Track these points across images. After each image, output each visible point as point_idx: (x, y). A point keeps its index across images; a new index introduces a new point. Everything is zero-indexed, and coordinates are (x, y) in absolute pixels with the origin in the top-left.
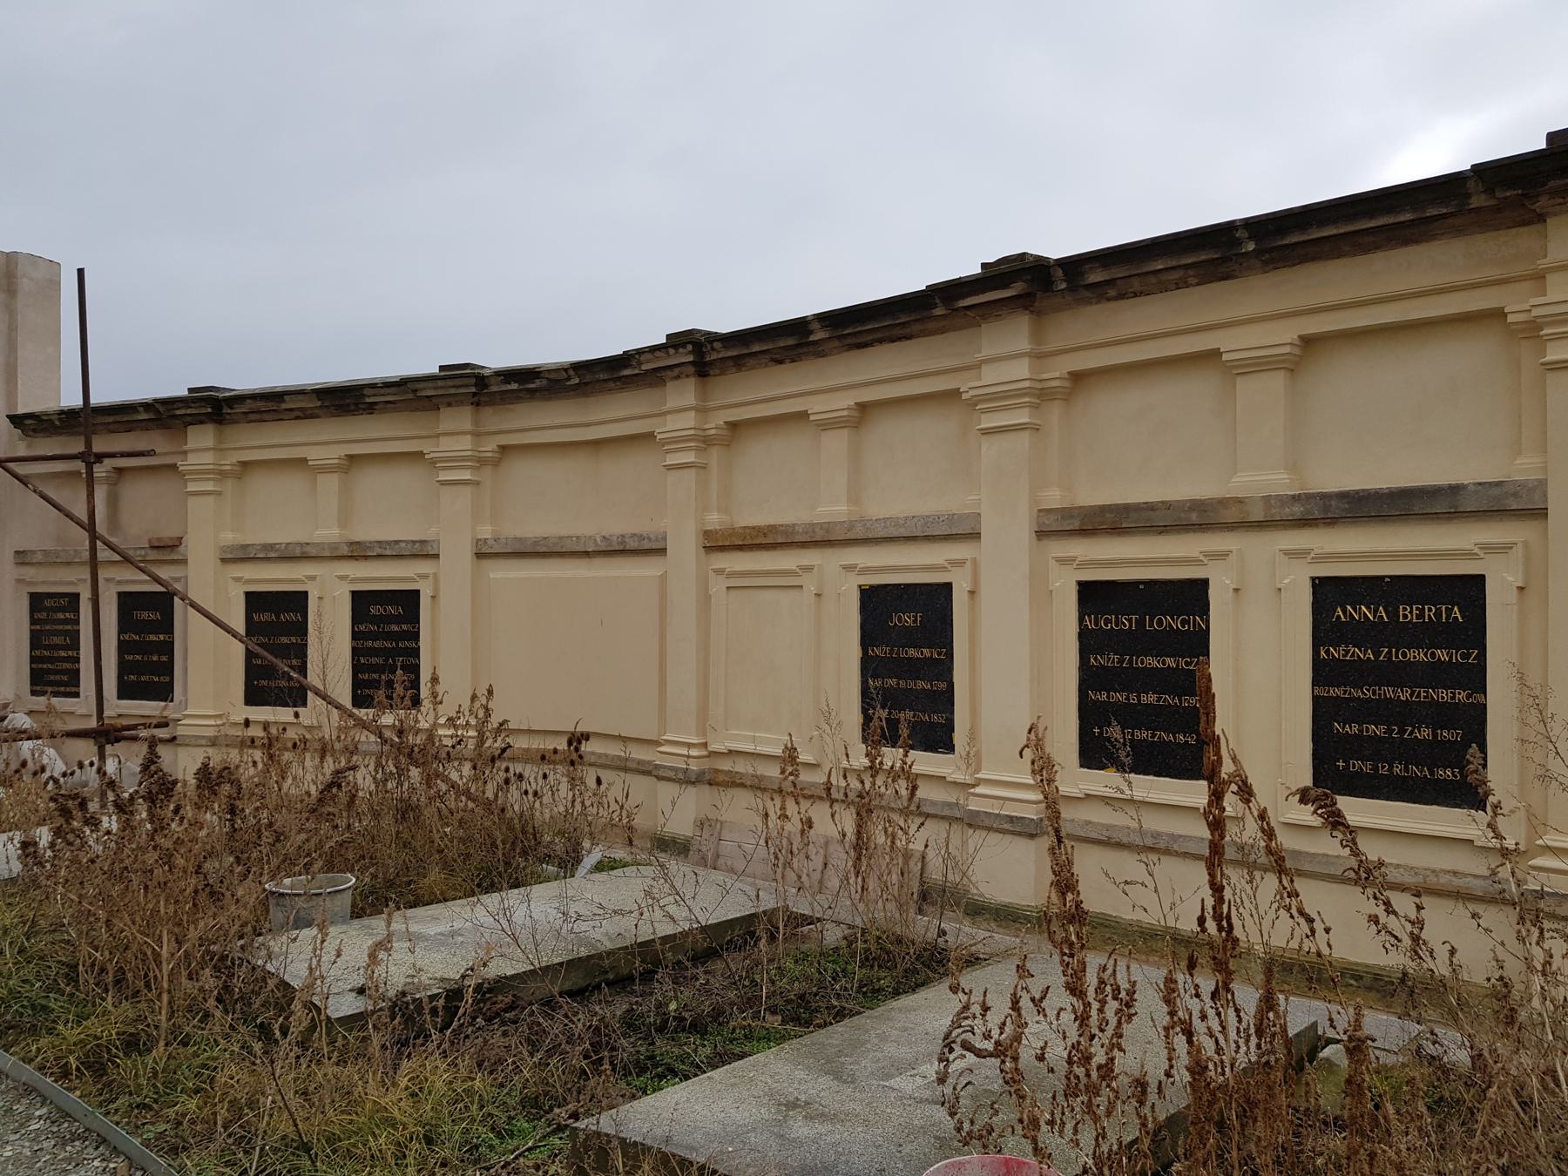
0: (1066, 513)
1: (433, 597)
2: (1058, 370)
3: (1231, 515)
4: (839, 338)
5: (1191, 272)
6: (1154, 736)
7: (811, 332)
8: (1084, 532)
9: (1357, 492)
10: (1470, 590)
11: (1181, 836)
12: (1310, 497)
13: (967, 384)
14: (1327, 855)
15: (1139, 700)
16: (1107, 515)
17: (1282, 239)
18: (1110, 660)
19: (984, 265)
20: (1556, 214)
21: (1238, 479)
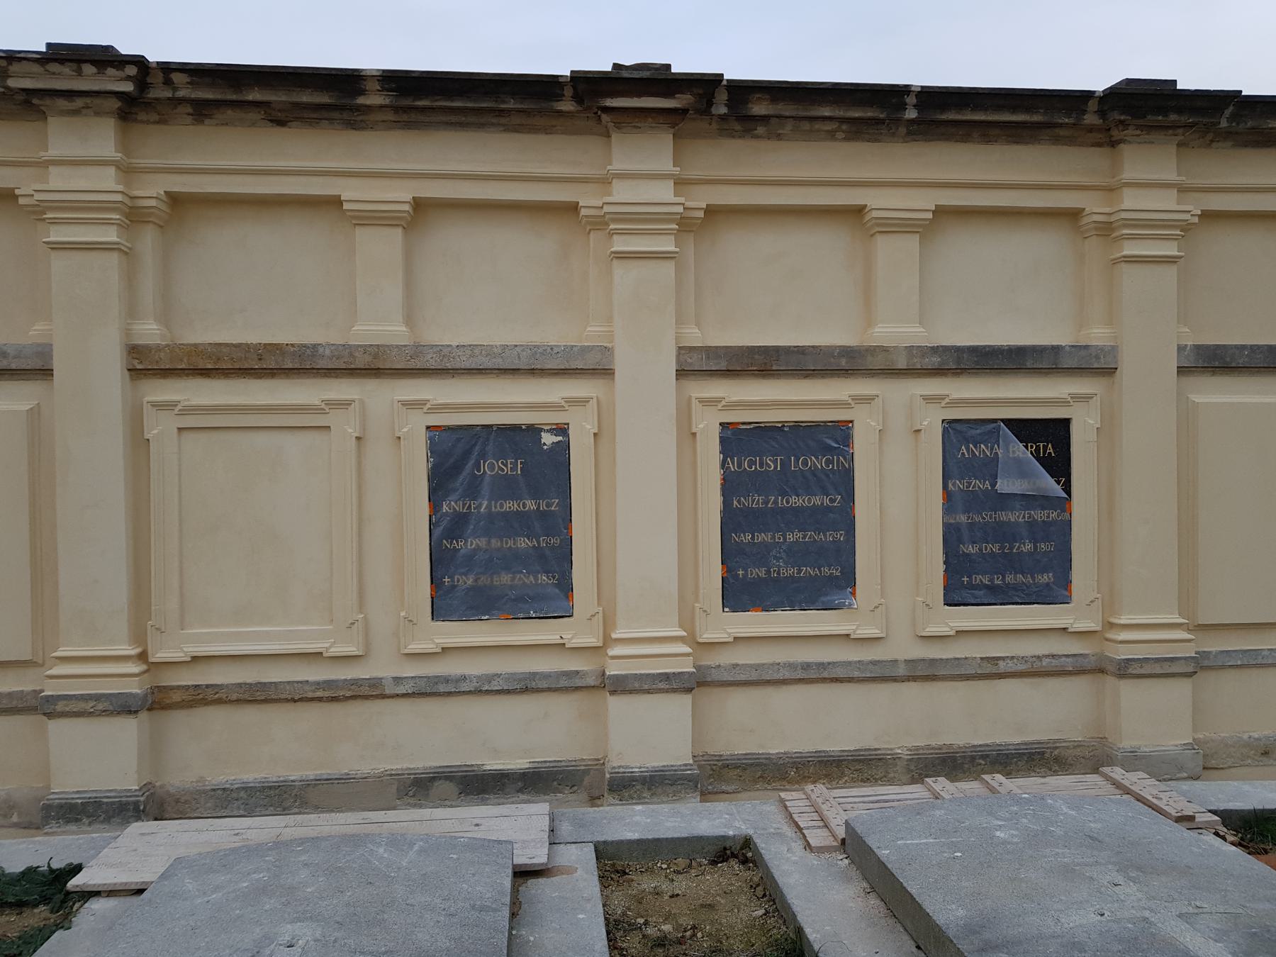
0: (711, 352)
1: (358, 438)
3: (877, 362)
4: (396, 109)
5: (844, 127)
6: (799, 571)
7: (362, 92)
8: (729, 373)
9: (985, 347)
10: (841, 433)
11: (829, 663)
12: (946, 349)
13: (588, 200)
14: (958, 659)
15: (785, 539)
16: (756, 357)
17: (941, 113)
18: (755, 501)
19: (616, 66)
20: (1130, 142)
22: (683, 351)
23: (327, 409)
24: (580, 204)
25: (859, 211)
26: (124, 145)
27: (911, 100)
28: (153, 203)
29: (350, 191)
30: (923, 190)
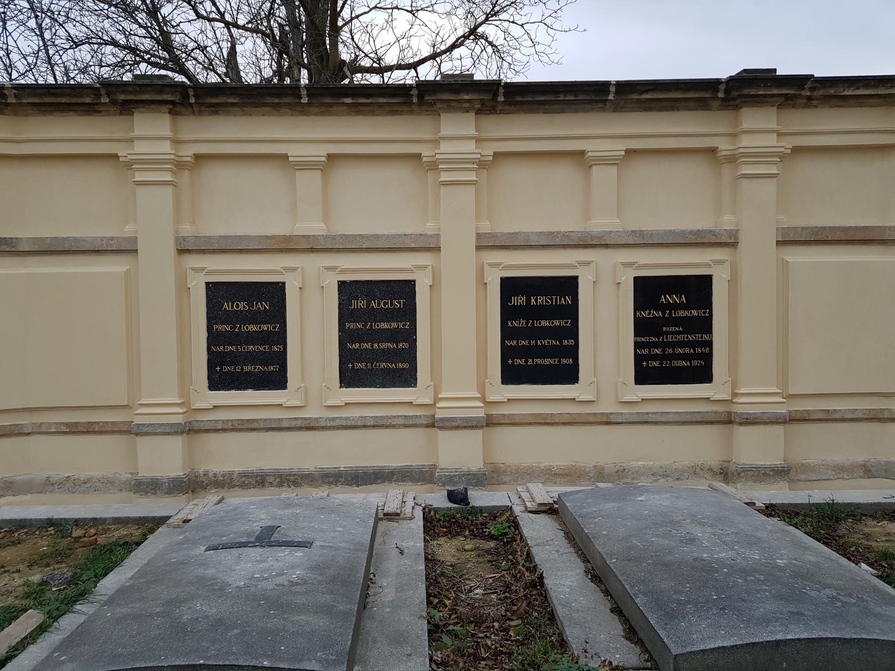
2: (489, 150)
21: (430, 224)
22: (479, 236)
23: (284, 271)
24: (423, 155)
25: (582, 153)
26: (174, 128)
27: (612, 89)
28: (189, 159)
29: (294, 151)
30: (618, 140)
